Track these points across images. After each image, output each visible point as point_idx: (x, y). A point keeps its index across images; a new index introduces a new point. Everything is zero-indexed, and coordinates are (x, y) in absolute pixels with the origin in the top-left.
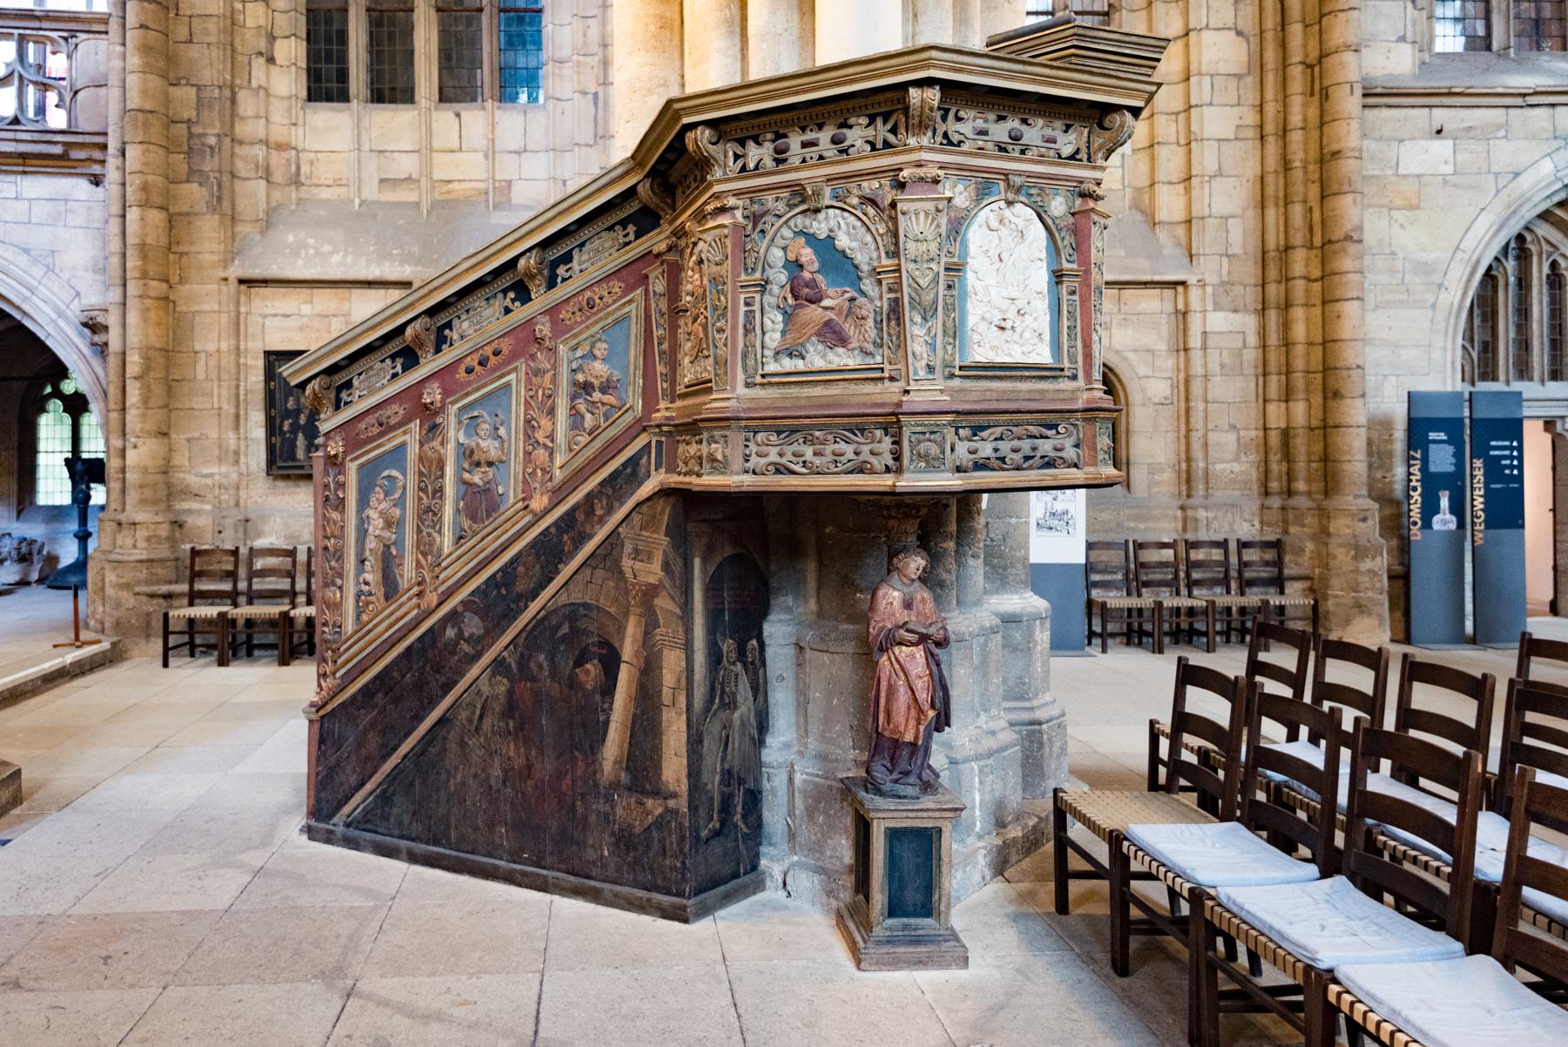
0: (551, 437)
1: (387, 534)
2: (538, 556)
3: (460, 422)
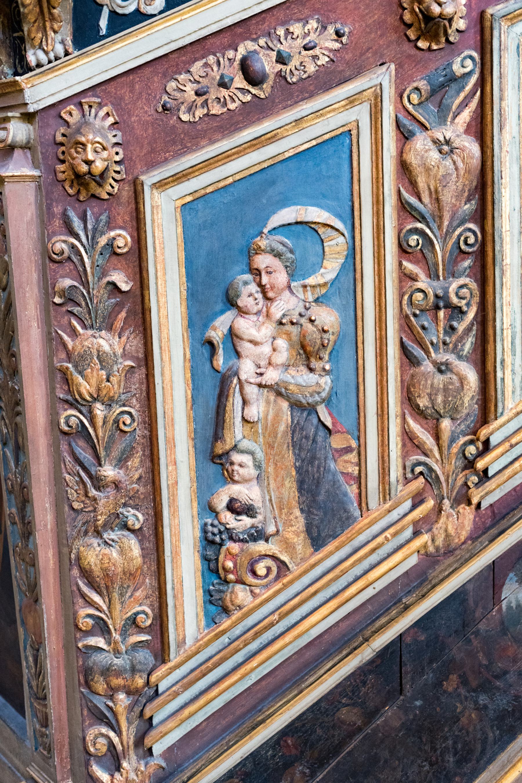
1: (301, 379)
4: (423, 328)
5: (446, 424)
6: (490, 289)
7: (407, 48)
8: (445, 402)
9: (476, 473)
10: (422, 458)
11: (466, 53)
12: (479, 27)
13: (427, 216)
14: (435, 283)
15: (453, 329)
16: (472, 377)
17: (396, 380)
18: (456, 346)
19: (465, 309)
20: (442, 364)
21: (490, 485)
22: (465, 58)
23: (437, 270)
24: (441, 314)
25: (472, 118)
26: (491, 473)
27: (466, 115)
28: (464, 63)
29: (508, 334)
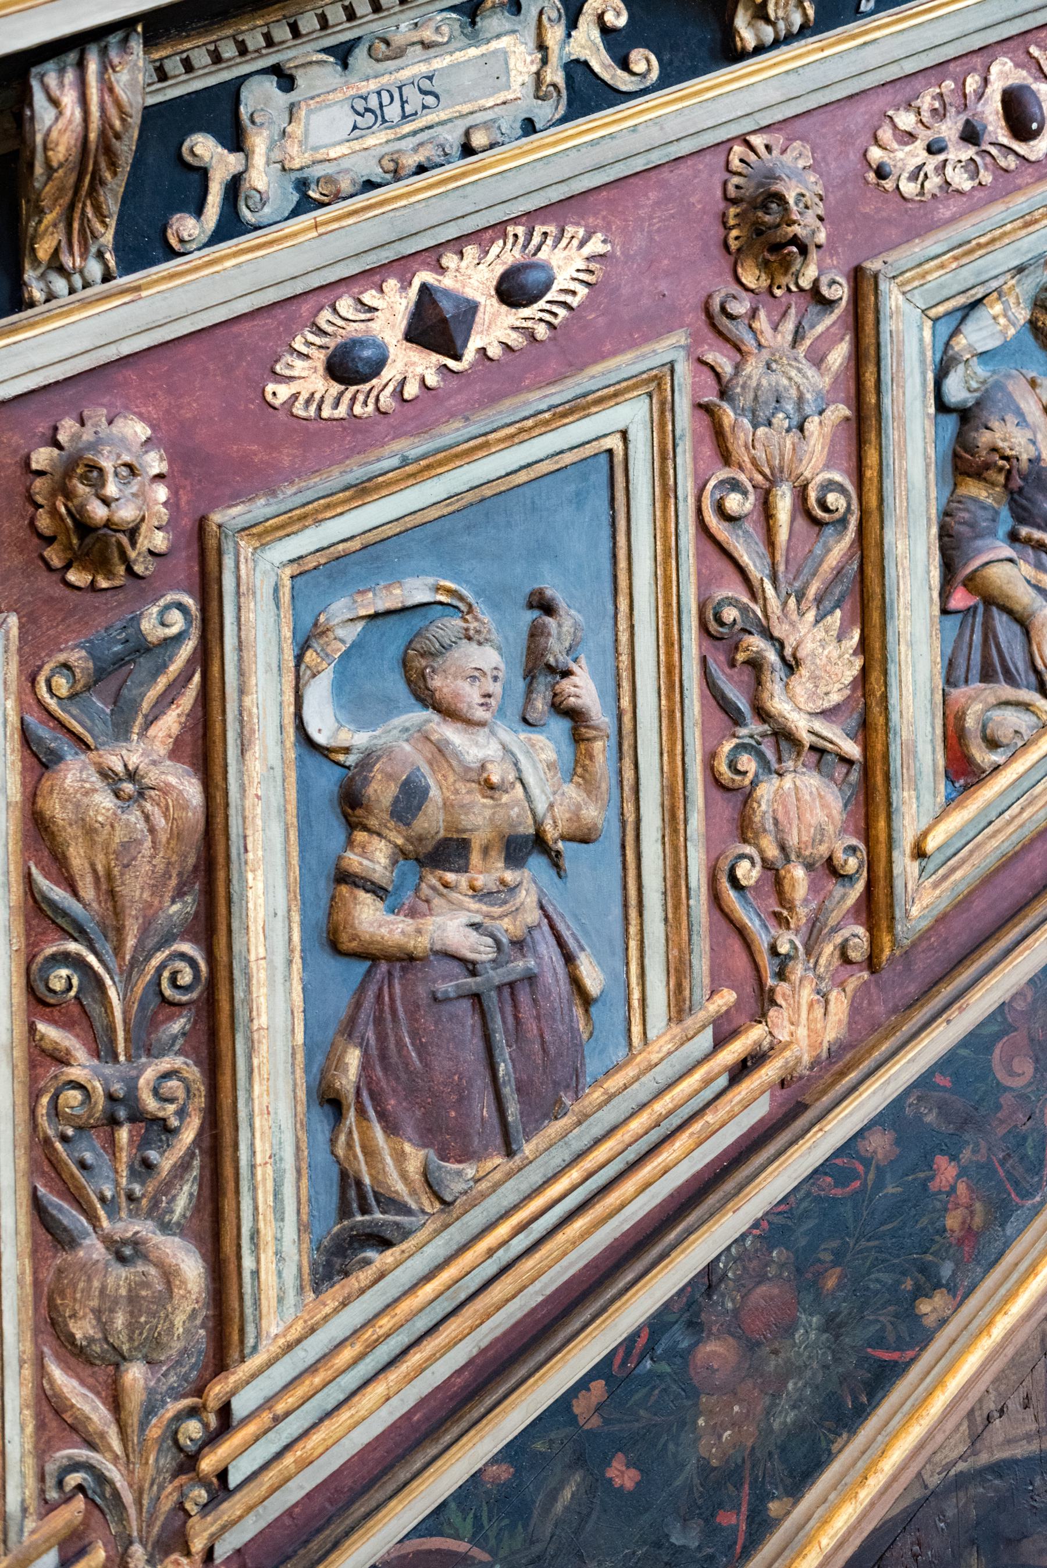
0: (868, 705)
2: (804, 1275)
3: (307, 640)
4: (83, 1165)
5: (135, 1374)
6: (226, 1081)
7: (45, 582)
8: (132, 1326)
9: (203, 1481)
10: (83, 1454)
11: (169, 598)
12: (195, 548)
13: (90, 927)
14: (108, 1070)
15: (148, 1166)
16: (191, 1268)
17: (20, 1282)
18: (155, 1203)
19: (174, 1122)
20: (124, 1242)
21: (232, 1508)
22: (167, 607)
23: (112, 1041)
24: (123, 1134)
25: (184, 727)
26: (233, 1481)
27: (171, 722)
28: (166, 618)
29: (265, 1175)
